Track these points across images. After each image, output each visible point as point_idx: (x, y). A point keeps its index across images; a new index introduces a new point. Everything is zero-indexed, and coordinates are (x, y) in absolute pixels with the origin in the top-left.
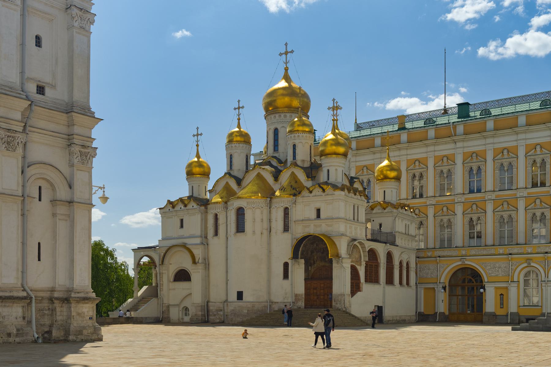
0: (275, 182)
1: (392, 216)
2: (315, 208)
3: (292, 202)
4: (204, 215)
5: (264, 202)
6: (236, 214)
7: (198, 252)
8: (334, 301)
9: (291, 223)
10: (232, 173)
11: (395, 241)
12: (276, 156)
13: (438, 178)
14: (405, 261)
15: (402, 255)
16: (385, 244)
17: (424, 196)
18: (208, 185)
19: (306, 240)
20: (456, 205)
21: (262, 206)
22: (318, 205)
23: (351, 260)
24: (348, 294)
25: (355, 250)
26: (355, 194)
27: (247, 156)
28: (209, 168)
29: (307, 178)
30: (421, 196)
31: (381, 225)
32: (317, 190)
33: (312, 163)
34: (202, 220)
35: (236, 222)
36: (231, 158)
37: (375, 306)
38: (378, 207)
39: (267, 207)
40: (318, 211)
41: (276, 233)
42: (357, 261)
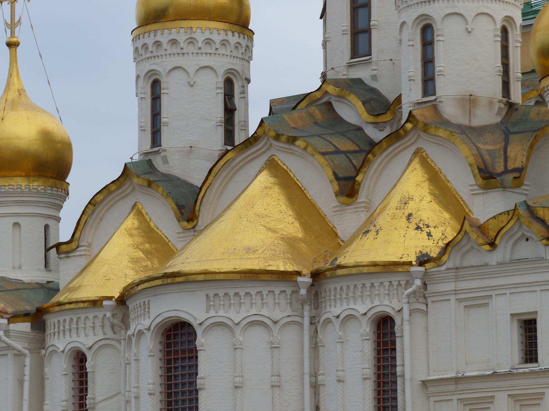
0: (344, 199)
2: (513, 315)
3: (406, 292)
4: (28, 361)
5: (283, 295)
6: (159, 355)
9: (404, 391)
10: (158, 163)
12: (359, 82)
18: (58, 219)
21: (277, 314)
27: (229, 83)
28: (67, 146)
29: (480, 181)
32: (519, 235)
33: (511, 106)
34: (21, 382)
35: (159, 389)
36: (156, 99)
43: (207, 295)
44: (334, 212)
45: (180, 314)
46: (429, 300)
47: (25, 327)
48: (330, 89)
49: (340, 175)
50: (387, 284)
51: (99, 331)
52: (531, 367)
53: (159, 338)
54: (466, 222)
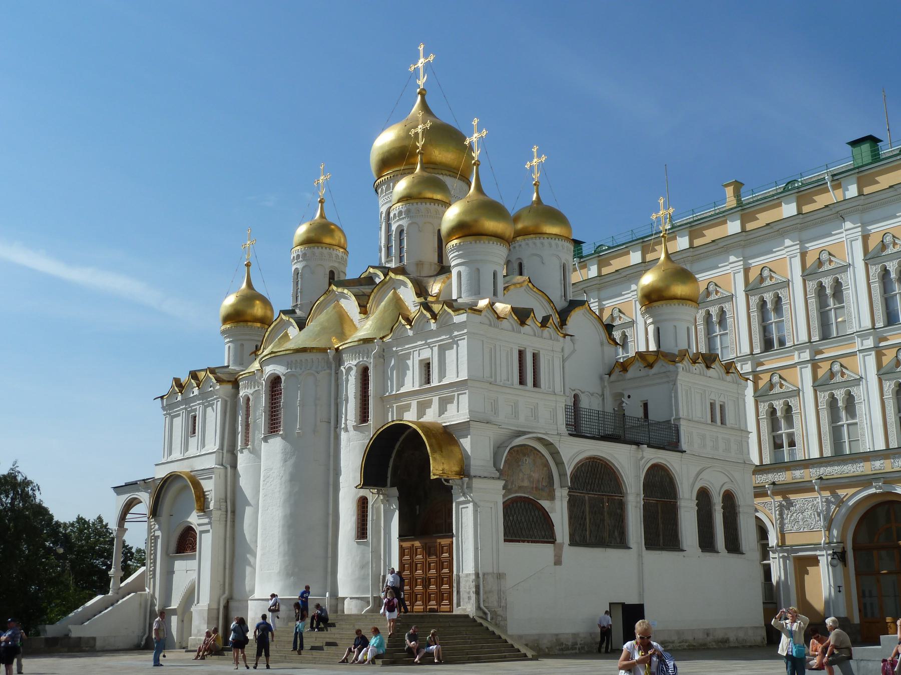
0: (363, 316)
1: (668, 382)
2: (421, 361)
4: (229, 403)
7: (208, 486)
8: (458, 592)
10: (297, 311)
11: (679, 442)
13: (814, 300)
14: (718, 491)
15: (704, 475)
16: (634, 447)
17: (788, 345)
19: (401, 439)
20: (860, 356)
22: (426, 354)
23: (503, 482)
24: (495, 572)
25: (528, 460)
26: (523, 323)
30: (782, 343)
31: (646, 406)
37: (610, 604)
38: (639, 364)
39: (328, 371)
40: (427, 366)
41: (346, 430)
42: (536, 488)
43: (288, 362)
44: (359, 322)
45: (276, 372)
46: (385, 356)
47: (229, 387)
48: (371, 270)
49: (361, 304)
50: (366, 351)
51: (256, 387)
52: (428, 386)
53: (269, 384)
54: (400, 316)
